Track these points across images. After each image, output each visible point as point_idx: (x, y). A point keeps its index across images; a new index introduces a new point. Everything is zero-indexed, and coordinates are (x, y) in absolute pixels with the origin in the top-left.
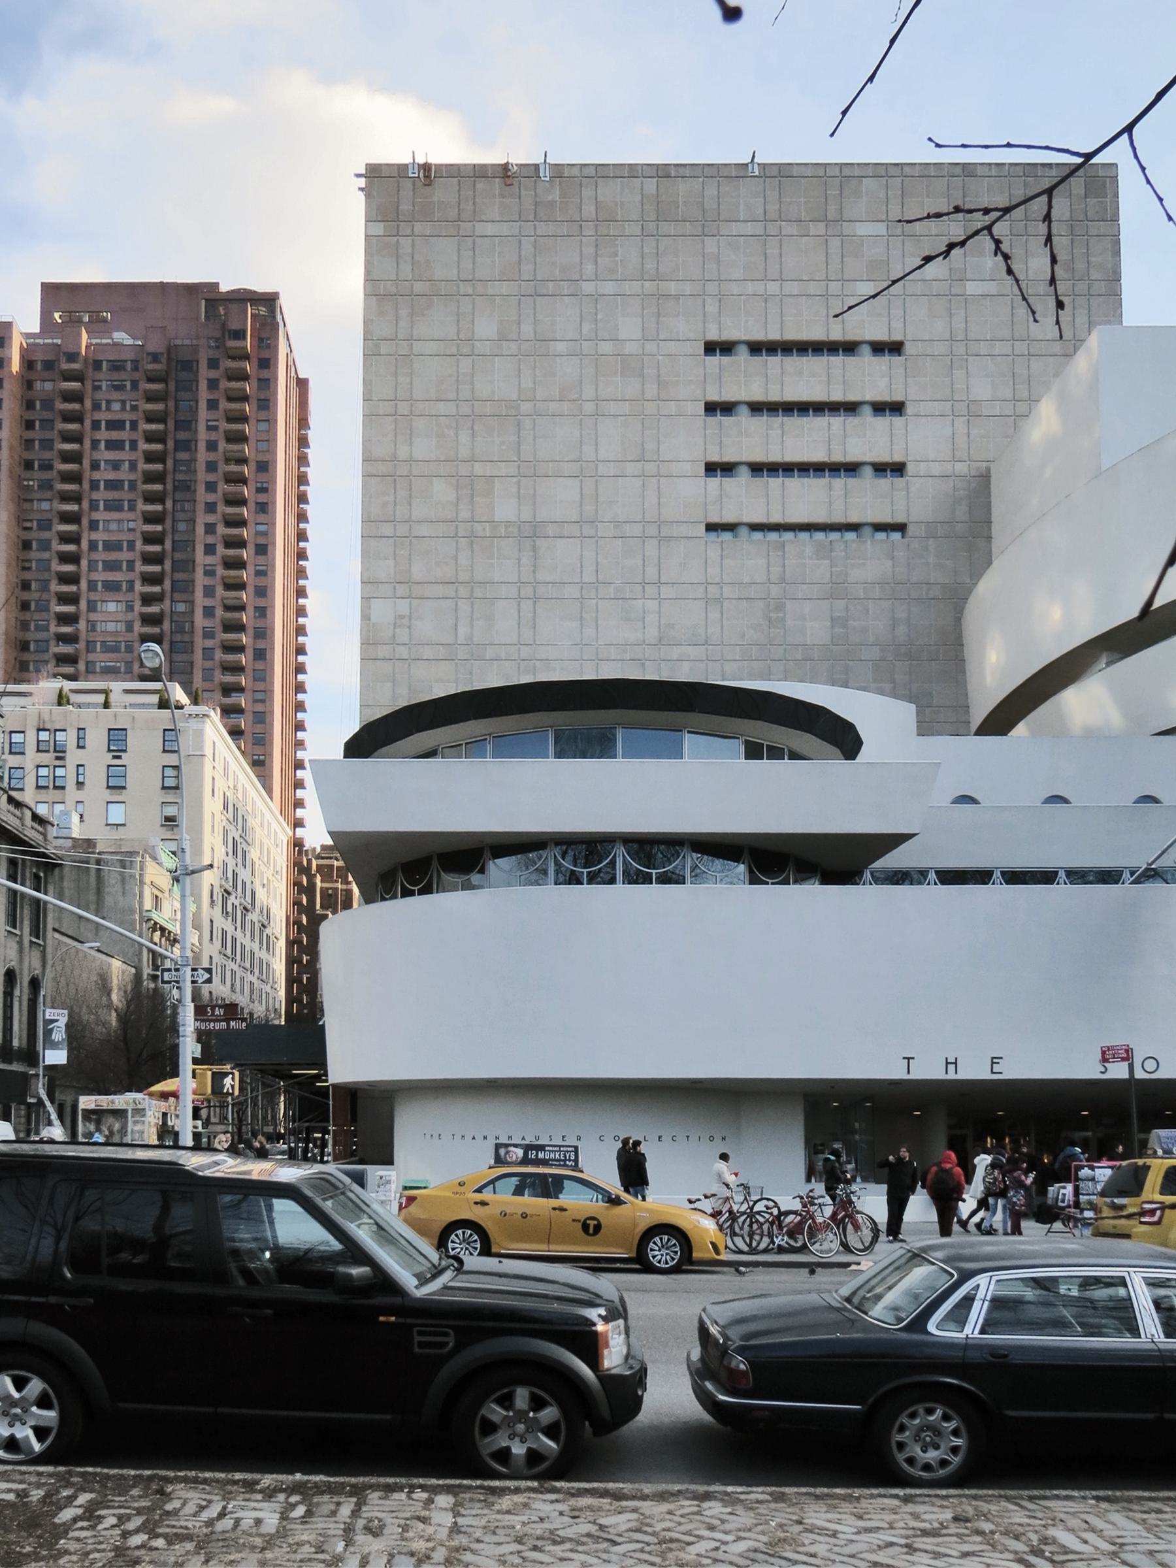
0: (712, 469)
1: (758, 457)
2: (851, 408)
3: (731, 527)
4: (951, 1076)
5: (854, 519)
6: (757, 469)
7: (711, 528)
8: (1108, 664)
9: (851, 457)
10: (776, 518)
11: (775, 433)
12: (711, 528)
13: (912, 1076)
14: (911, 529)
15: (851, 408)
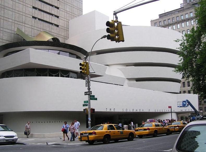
0: (34, 7)
1: (40, 8)
2: (52, 6)
3: (35, 18)
4: (110, 111)
5: (53, 22)
6: (40, 10)
7: (33, 17)
8: (97, 55)
9: (53, 13)
10: (42, 19)
11: (42, 6)
12: (33, 17)
13: (107, 111)
14: (59, 26)
15: (52, 6)
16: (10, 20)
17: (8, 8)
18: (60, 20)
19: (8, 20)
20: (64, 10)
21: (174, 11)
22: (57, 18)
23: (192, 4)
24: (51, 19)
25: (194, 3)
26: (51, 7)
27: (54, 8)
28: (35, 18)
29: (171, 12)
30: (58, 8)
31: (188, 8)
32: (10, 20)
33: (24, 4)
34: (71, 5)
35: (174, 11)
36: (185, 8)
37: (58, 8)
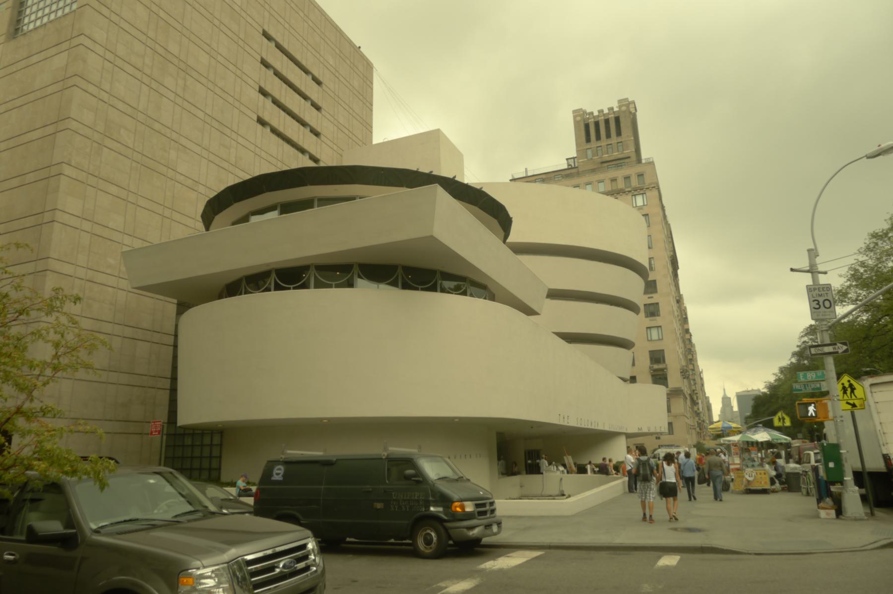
9: (307, 118)
16: (200, 114)
17: (194, 74)
18: (324, 145)
19: (193, 110)
20: (332, 119)
21: (553, 175)
22: (315, 137)
23: (600, 160)
24: (301, 137)
25: (604, 160)
26: (303, 100)
27: (308, 104)
28: (261, 122)
29: (544, 176)
30: (318, 108)
31: (593, 171)
32: (200, 114)
33: (239, 73)
34: (347, 108)
35: (553, 175)
36: (581, 169)
37: (318, 108)
